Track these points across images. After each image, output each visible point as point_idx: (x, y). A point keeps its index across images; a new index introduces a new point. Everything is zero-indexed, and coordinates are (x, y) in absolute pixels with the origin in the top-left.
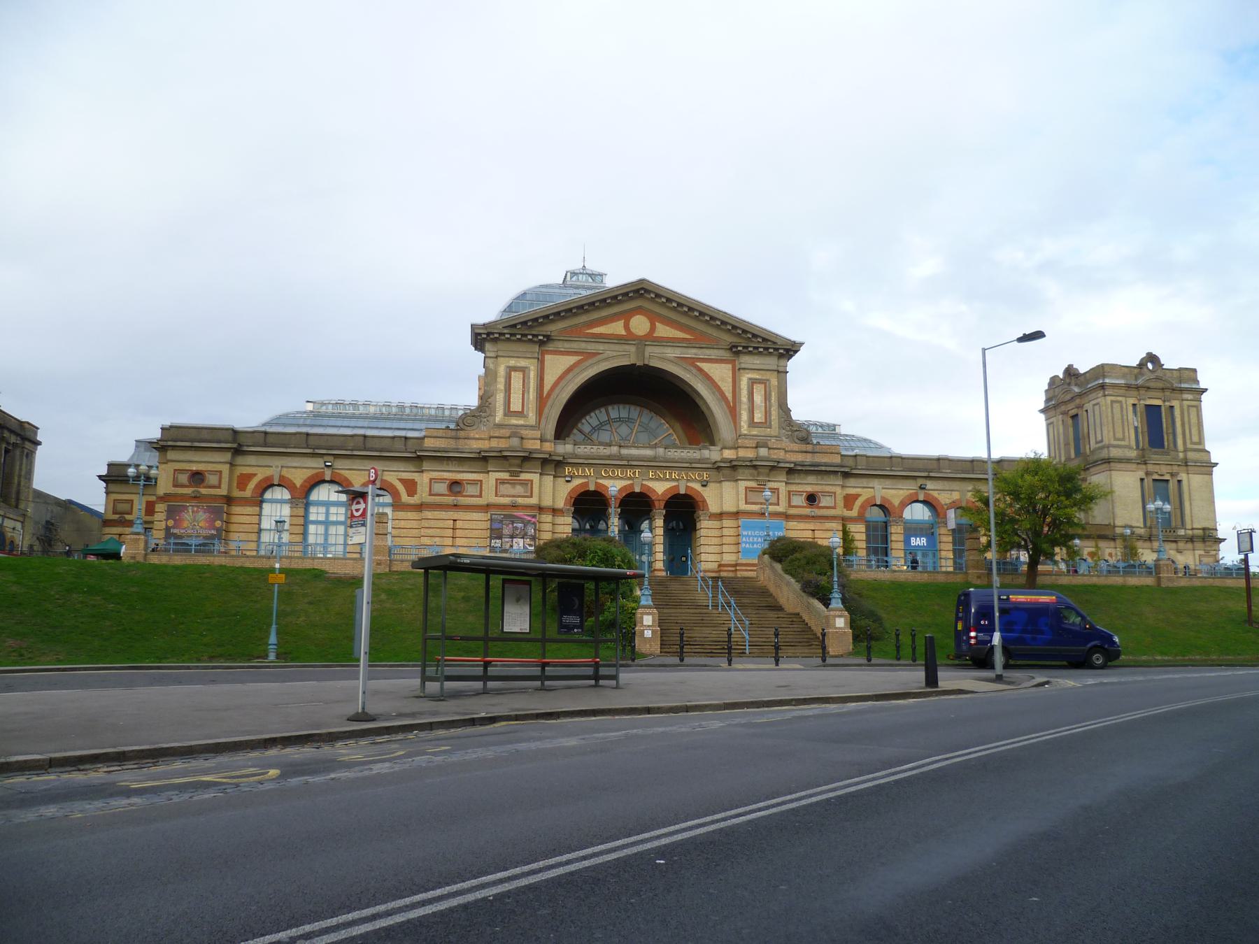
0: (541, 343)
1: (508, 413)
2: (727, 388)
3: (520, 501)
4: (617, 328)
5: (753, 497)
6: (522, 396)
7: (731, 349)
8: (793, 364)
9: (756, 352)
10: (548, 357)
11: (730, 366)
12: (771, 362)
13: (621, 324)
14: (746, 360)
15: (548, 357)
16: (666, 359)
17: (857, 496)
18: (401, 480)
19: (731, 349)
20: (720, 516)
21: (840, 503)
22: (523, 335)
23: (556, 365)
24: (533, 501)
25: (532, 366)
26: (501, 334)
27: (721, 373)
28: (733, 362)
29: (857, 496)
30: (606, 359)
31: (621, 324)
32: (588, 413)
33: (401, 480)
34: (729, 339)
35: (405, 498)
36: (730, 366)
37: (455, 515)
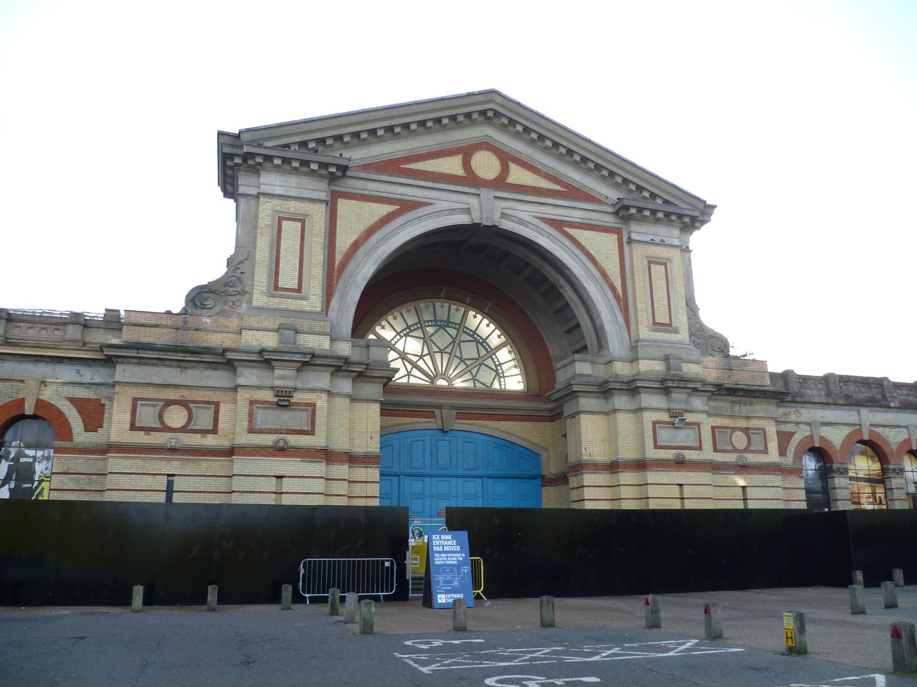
0: (333, 178)
1: (276, 288)
2: (613, 269)
3: (294, 440)
4: (452, 165)
5: (665, 435)
6: (300, 260)
7: (616, 213)
8: (697, 239)
9: (654, 218)
10: (343, 205)
11: (615, 236)
12: (672, 234)
13: (458, 160)
14: (639, 231)
15: (343, 205)
16: (525, 219)
18: (73, 401)
19: (616, 213)
20: (613, 467)
21: (773, 446)
22: (305, 163)
23: (355, 217)
24: (317, 441)
25: (318, 215)
26: (268, 158)
27: (603, 246)
28: (618, 231)
29: (792, 434)
30: (439, 213)
31: (458, 160)
32: (393, 308)
33: (73, 401)
34: (613, 195)
35: (80, 435)
36: (615, 236)
37: (172, 466)
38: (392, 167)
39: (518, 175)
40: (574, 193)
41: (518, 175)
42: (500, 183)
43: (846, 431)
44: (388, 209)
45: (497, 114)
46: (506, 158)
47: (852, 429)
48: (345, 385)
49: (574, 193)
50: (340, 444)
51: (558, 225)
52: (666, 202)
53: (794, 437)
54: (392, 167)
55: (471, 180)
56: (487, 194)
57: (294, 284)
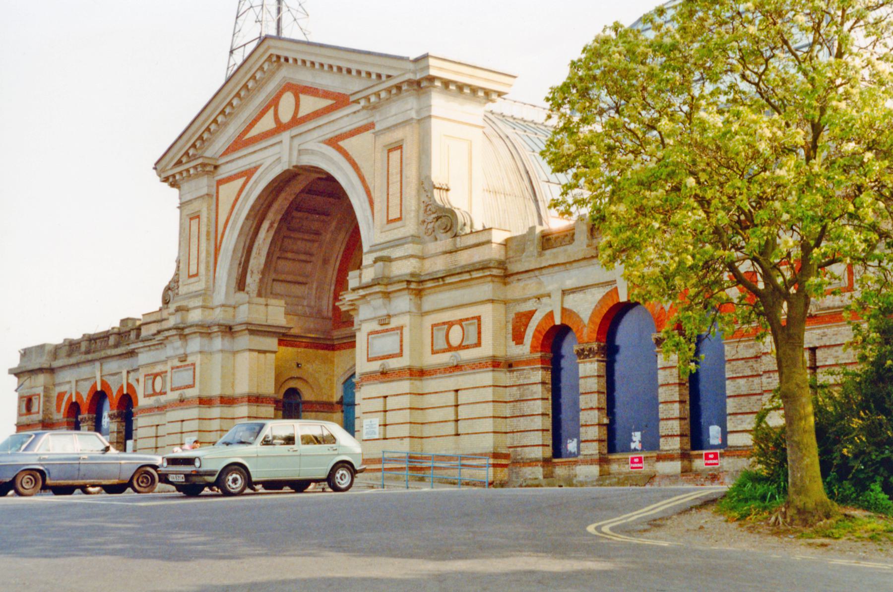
12: (408, 105)
17: (530, 315)
29: (530, 315)
38: (240, 143)
39: (309, 105)
40: (341, 101)
41: (309, 105)
42: (296, 121)
43: (598, 294)
44: (241, 181)
45: (278, 57)
46: (299, 90)
47: (608, 289)
48: (218, 343)
49: (341, 101)
50: (216, 391)
51: (333, 142)
52: (389, 76)
53: (534, 318)
54: (240, 143)
55: (280, 128)
56: (285, 136)
57: (195, 272)
